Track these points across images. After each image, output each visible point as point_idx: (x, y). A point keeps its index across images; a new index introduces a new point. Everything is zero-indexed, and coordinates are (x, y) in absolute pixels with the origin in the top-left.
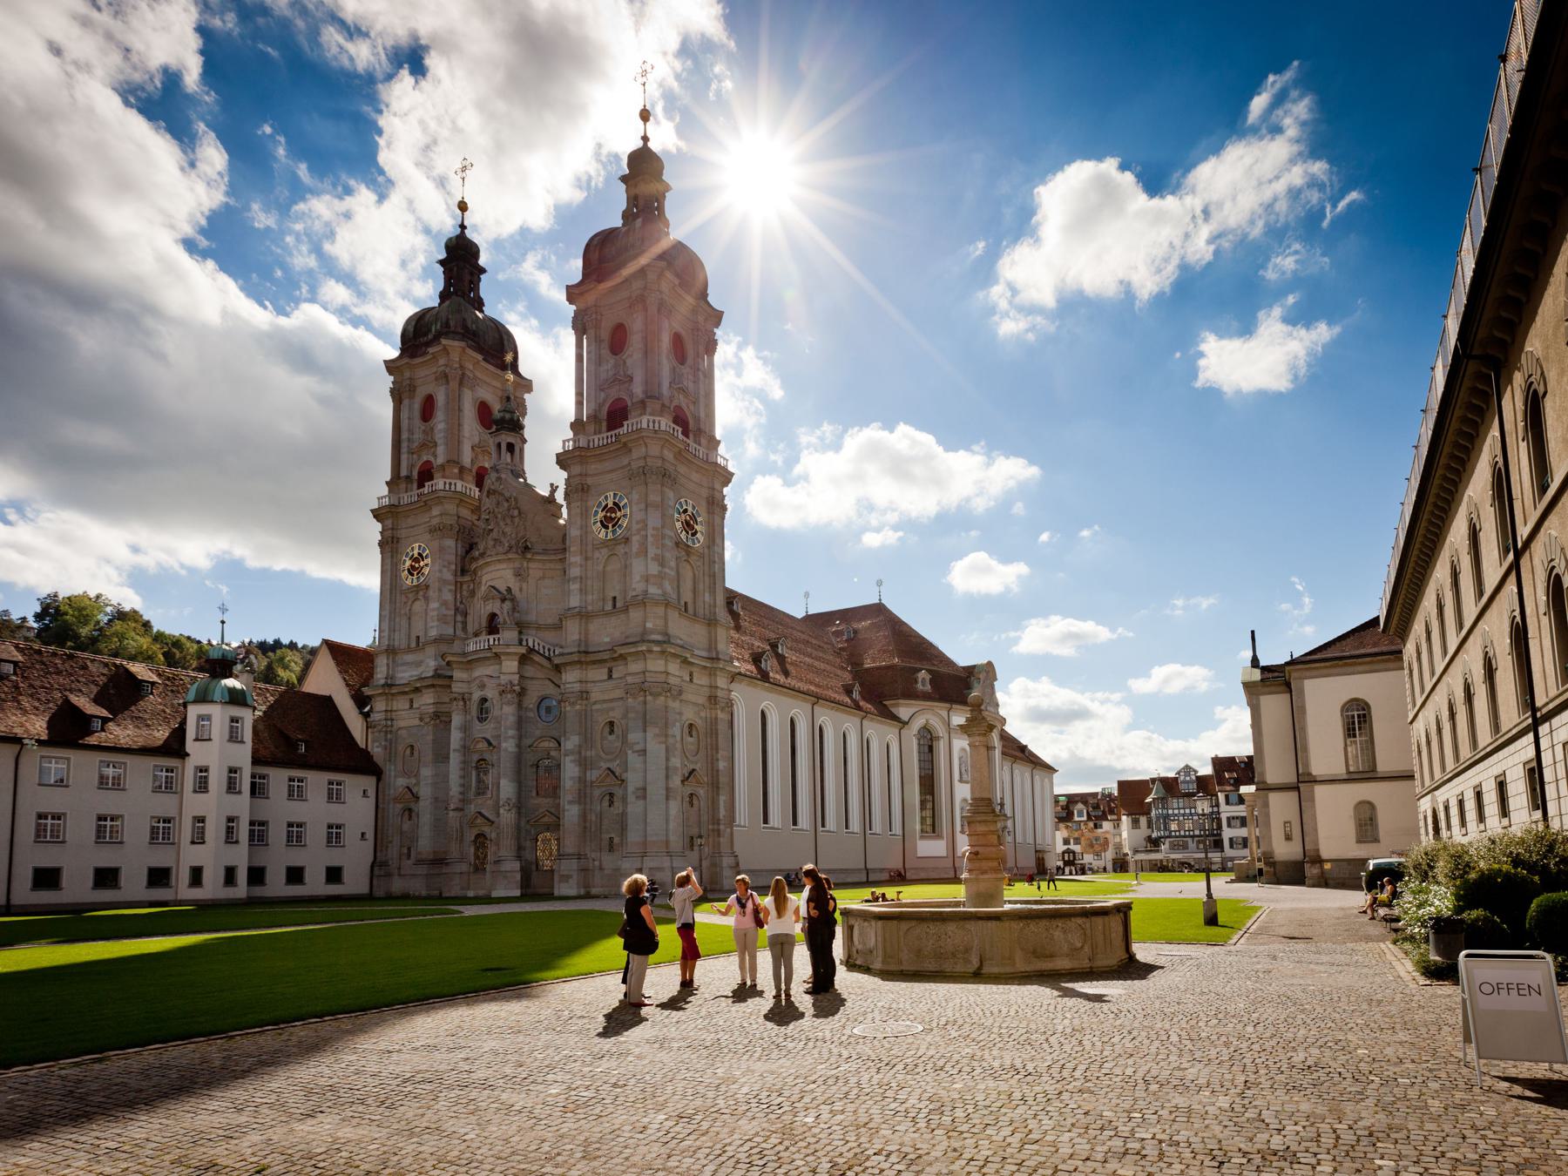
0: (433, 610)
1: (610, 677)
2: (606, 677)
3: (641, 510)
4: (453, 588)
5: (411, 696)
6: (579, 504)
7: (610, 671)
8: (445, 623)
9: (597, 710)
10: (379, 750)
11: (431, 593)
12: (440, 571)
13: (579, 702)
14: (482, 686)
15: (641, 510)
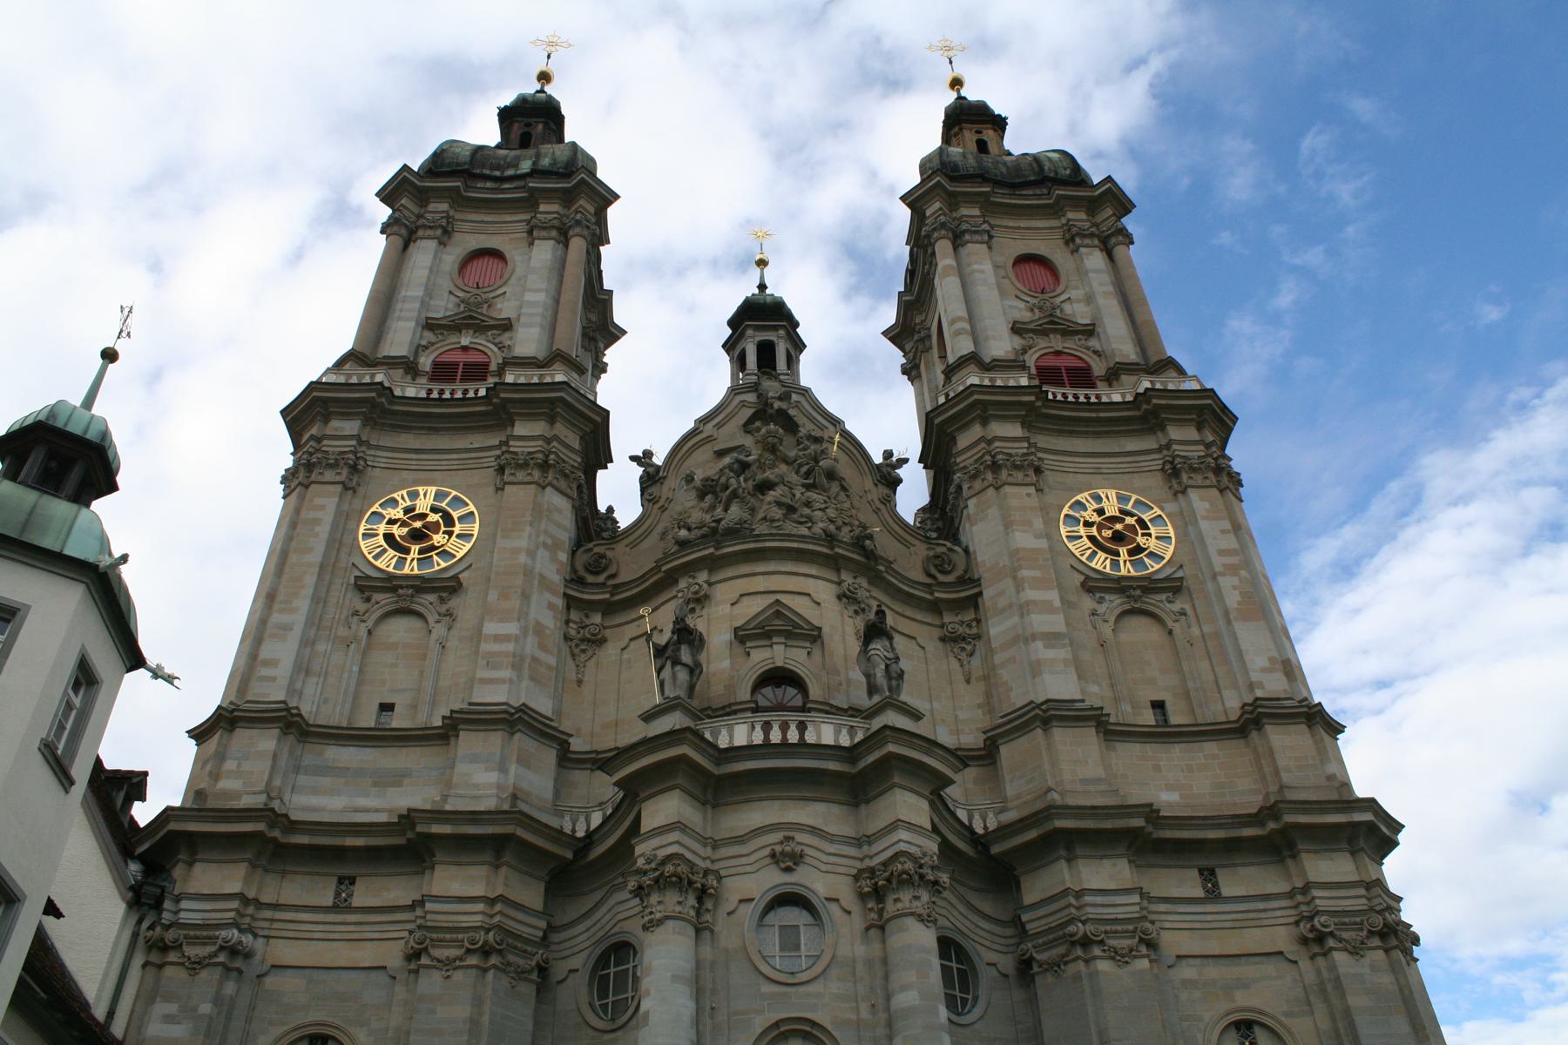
0: (497, 638)
1: (1213, 895)
2: (1199, 892)
3: (1223, 532)
4: (560, 602)
5: (347, 871)
6: (1032, 490)
7: (1208, 875)
8: (532, 678)
9: (1188, 984)
10: (178, 1031)
11: (466, 607)
12: (531, 553)
13: (1144, 950)
14: (788, 859)
15: (1223, 532)
